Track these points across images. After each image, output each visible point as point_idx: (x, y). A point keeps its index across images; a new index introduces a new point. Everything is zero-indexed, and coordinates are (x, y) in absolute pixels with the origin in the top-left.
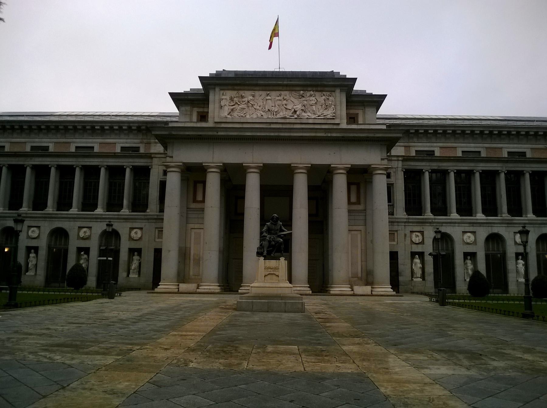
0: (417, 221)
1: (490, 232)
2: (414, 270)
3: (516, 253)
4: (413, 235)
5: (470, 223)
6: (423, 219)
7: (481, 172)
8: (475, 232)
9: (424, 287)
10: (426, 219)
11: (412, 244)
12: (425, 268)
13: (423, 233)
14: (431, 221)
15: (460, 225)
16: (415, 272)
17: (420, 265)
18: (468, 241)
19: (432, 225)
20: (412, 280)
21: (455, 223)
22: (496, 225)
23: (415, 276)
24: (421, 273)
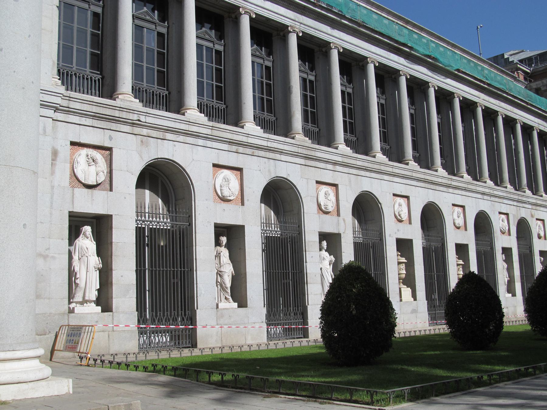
0: (95, 109)
1: (273, 175)
2: (78, 276)
3: (319, 232)
4: (79, 155)
5: (231, 142)
6: (114, 107)
7: (254, 16)
8: (240, 170)
9: (107, 333)
10: (121, 109)
11: (73, 187)
12: (111, 270)
13: (111, 155)
14: (135, 117)
15: (209, 143)
16: (81, 281)
17: (95, 261)
18: (226, 193)
19: (137, 130)
20: (71, 311)
21: (196, 136)
22: (283, 158)
23: (78, 297)
24: (98, 287)
